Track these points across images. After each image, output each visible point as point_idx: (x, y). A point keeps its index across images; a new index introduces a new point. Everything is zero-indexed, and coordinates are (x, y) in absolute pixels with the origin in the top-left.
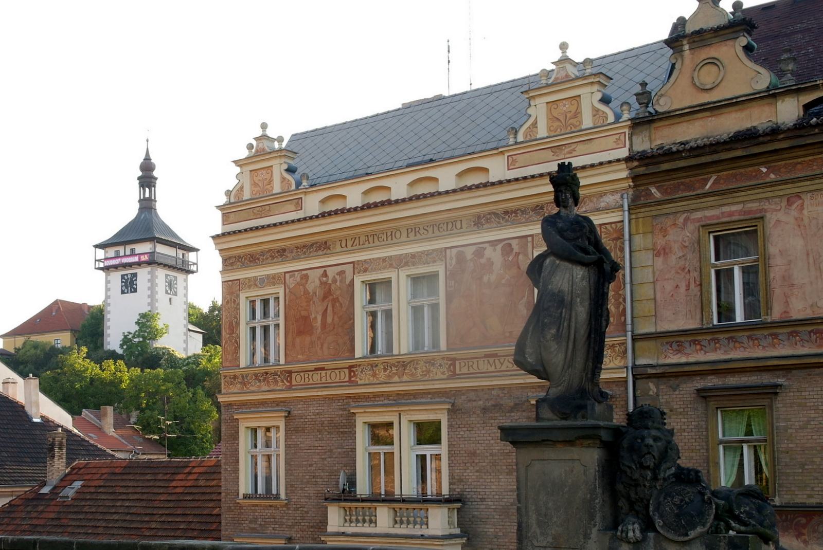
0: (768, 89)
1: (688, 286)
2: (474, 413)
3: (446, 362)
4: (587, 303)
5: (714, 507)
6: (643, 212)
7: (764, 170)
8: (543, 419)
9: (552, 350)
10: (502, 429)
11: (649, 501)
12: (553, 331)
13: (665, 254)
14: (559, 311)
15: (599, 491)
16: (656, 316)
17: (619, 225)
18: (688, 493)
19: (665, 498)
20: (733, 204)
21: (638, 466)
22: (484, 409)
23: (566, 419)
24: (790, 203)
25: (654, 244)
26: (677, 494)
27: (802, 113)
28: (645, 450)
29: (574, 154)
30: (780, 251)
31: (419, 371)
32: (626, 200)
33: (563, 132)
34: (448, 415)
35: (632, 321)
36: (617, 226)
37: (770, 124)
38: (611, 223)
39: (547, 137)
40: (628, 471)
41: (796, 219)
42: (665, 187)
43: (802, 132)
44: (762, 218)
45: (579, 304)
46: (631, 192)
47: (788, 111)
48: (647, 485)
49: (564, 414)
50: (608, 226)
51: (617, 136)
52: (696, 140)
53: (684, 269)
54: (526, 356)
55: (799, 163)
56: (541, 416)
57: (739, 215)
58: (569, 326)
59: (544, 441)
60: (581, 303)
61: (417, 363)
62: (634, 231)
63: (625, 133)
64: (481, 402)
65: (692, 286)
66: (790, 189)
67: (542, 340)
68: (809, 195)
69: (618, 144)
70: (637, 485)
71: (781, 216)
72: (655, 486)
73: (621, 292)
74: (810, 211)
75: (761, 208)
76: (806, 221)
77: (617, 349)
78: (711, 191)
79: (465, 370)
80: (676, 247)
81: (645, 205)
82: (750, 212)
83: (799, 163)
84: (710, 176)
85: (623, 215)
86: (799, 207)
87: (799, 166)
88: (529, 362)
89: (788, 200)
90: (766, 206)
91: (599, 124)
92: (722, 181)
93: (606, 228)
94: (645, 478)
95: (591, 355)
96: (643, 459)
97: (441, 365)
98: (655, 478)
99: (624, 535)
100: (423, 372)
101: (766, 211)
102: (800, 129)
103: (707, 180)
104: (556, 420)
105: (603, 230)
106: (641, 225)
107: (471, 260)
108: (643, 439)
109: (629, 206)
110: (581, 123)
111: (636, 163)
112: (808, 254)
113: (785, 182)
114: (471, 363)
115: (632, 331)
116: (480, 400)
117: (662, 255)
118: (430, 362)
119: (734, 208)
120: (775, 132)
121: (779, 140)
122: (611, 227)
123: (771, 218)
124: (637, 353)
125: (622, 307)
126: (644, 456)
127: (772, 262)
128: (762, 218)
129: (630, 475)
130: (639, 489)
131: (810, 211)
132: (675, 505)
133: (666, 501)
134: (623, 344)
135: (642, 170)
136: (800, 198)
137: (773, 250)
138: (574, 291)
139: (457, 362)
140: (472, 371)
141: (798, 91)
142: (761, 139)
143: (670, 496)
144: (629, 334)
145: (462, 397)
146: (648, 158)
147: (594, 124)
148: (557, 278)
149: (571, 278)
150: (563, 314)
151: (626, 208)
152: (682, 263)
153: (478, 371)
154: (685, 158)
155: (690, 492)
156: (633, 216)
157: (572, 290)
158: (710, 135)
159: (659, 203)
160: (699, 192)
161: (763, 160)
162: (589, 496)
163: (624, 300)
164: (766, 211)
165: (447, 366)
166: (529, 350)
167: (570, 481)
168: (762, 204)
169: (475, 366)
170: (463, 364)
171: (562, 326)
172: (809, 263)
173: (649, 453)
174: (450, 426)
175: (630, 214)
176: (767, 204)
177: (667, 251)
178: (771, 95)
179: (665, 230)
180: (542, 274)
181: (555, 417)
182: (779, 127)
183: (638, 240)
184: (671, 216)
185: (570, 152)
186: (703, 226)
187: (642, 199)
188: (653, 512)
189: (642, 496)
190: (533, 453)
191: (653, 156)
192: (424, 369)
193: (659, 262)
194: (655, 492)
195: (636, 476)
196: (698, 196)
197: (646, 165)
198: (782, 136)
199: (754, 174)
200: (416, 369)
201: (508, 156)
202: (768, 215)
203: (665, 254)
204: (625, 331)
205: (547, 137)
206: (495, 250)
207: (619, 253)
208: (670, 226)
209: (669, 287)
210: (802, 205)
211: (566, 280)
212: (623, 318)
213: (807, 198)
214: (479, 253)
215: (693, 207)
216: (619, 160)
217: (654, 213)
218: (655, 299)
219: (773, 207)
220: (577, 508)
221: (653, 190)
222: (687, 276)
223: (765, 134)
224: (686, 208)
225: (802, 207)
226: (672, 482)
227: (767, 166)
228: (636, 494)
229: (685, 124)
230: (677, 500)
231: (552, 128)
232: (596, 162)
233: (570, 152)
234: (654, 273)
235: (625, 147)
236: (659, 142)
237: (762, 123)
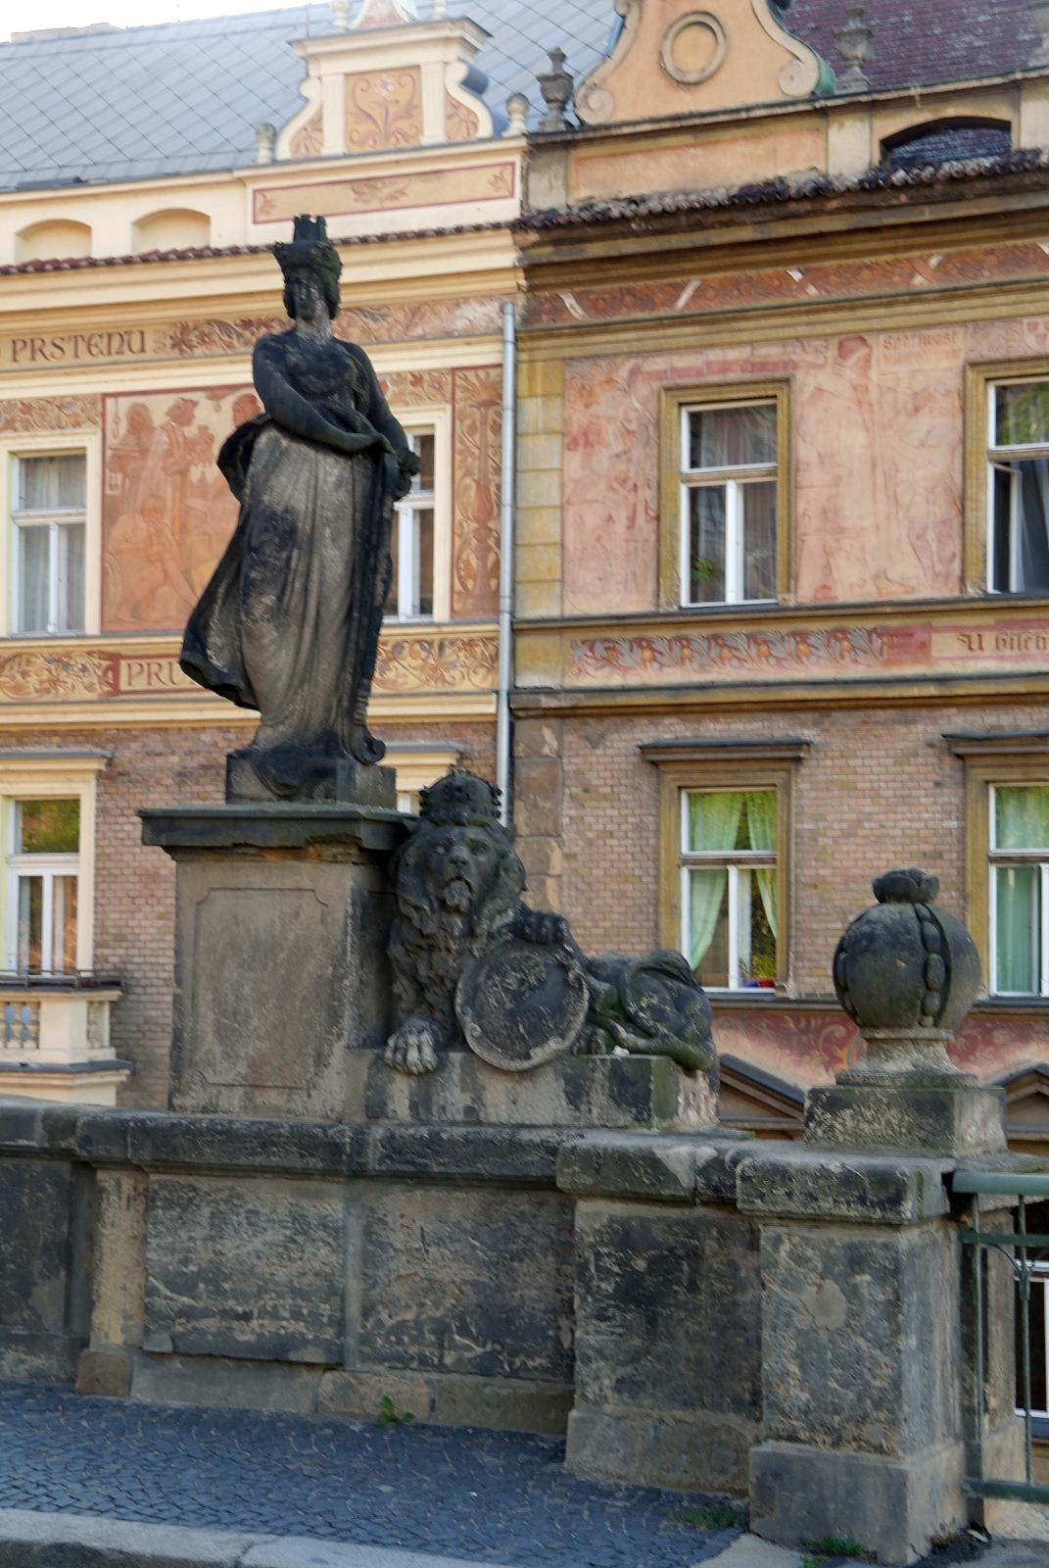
0: (813, 97)
1: (632, 520)
2: (158, 783)
3: (96, 661)
4: (346, 541)
5: (586, 995)
6: (547, 348)
7: (797, 276)
8: (240, 798)
9: (266, 641)
10: (147, 817)
11: (455, 983)
12: (269, 599)
13: (588, 444)
14: (284, 555)
15: (352, 959)
16: (562, 581)
17: (493, 372)
18: (537, 965)
19: (489, 977)
20: (732, 345)
21: (436, 905)
22: (180, 774)
23: (288, 798)
24: (843, 352)
25: (566, 422)
27: (877, 156)
28: (450, 871)
29: (403, 201)
30: (819, 455)
31: (33, 680)
32: (509, 318)
33: (379, 148)
34: (98, 785)
35: (513, 590)
36: (488, 374)
37: (813, 175)
38: (475, 368)
39: (345, 156)
40: (414, 915)
41: (855, 388)
42: (592, 297)
43: (875, 199)
44: (787, 381)
45: (328, 542)
46: (521, 300)
47: (850, 150)
48: (454, 947)
49: (288, 786)
50: (470, 375)
51: (497, 171)
52: (661, 196)
53: (624, 482)
54: (209, 652)
55: (868, 267)
56: (237, 790)
57: (743, 371)
58: (306, 589)
59: (237, 845)
60: (334, 540)
61: (29, 662)
62: (523, 389)
63: (513, 164)
64: (175, 759)
65: (641, 519)
66: (845, 322)
67: (244, 618)
68: (882, 337)
69: (498, 189)
70: (432, 948)
71: (824, 379)
73: (491, 525)
74: (883, 374)
75: (785, 358)
76: (874, 394)
77: (478, 649)
78: (687, 312)
79: (140, 683)
80: (610, 431)
81: (549, 334)
82: (763, 366)
83: (868, 267)
84: (685, 279)
85: (503, 352)
86: (861, 363)
87: (866, 274)
88: (215, 668)
89: (841, 346)
90: (797, 354)
91: (459, 139)
92: (710, 293)
93: (466, 379)
94: (448, 933)
95: (351, 658)
96: (446, 891)
97: (84, 669)
98: (471, 933)
100: (41, 682)
101: (795, 366)
102: (870, 191)
103: (679, 288)
104: (269, 800)
105: (459, 381)
106: (539, 379)
107: (163, 428)
108: (449, 845)
109: (516, 331)
110: (419, 130)
111: (533, 237)
112: (874, 466)
113: (836, 306)
114: (154, 668)
115: (512, 613)
116: (173, 753)
117: (581, 449)
118: (59, 661)
119: (732, 355)
120: (820, 193)
121: (830, 213)
122: (477, 376)
123: (806, 381)
124: (521, 660)
125: (492, 557)
126: (447, 884)
127: (804, 478)
128: (787, 381)
130: (436, 956)
131: (883, 374)
132: (506, 990)
134: (492, 639)
135: (546, 253)
136: (863, 340)
137: (805, 452)
138: (318, 511)
139: (123, 664)
140: (156, 685)
141: (873, 107)
142: (793, 207)
144: (506, 618)
145: (134, 745)
146: (559, 225)
147: (448, 136)
148: (283, 479)
149: (313, 482)
150: (293, 564)
151: (510, 335)
152: (622, 467)
153: (171, 686)
154: (636, 234)
155: (540, 961)
156: (524, 356)
157: (314, 510)
158: (689, 187)
159: (581, 330)
160: (662, 312)
161: (795, 253)
162: (330, 971)
163: (498, 543)
164: (795, 366)
165: (100, 673)
166: (215, 639)
167: (291, 936)
168: (790, 349)
169: (164, 675)
170: (136, 668)
171: (289, 588)
172: (874, 484)
173: (459, 878)
174: (102, 812)
175: (517, 349)
176: (799, 350)
177: (592, 438)
178: (820, 110)
179: (591, 393)
180: (251, 469)
181: (268, 794)
182: (830, 183)
183: (532, 409)
184: (603, 363)
185: (393, 197)
186: (668, 389)
187: (545, 317)
188: (462, 1007)
189: (441, 972)
190: (214, 873)
191: (570, 225)
192: (46, 675)
193: (575, 459)
194: (471, 963)
195: (431, 927)
196: (661, 323)
197: (556, 243)
198: (833, 204)
200: (24, 674)
201: (255, 192)
202: (800, 376)
203: (588, 444)
204: (497, 611)
205: (345, 156)
206: (218, 409)
207: (490, 436)
208: (600, 384)
209: (593, 518)
210: (867, 360)
211: (301, 485)
212: (493, 583)
213: (877, 344)
214: (182, 413)
215: (650, 344)
216: (497, 226)
217: (568, 352)
218: (562, 545)
219: (810, 358)
220: (304, 998)
221: (569, 301)
222: (631, 498)
223: (802, 197)
224: (636, 346)
225: (867, 363)
228: (431, 967)
229: (640, 158)
230: (512, 981)
231: (356, 137)
232: (449, 224)
233: (393, 197)
234: (563, 486)
235: (512, 195)
236: (583, 193)
237: (799, 172)
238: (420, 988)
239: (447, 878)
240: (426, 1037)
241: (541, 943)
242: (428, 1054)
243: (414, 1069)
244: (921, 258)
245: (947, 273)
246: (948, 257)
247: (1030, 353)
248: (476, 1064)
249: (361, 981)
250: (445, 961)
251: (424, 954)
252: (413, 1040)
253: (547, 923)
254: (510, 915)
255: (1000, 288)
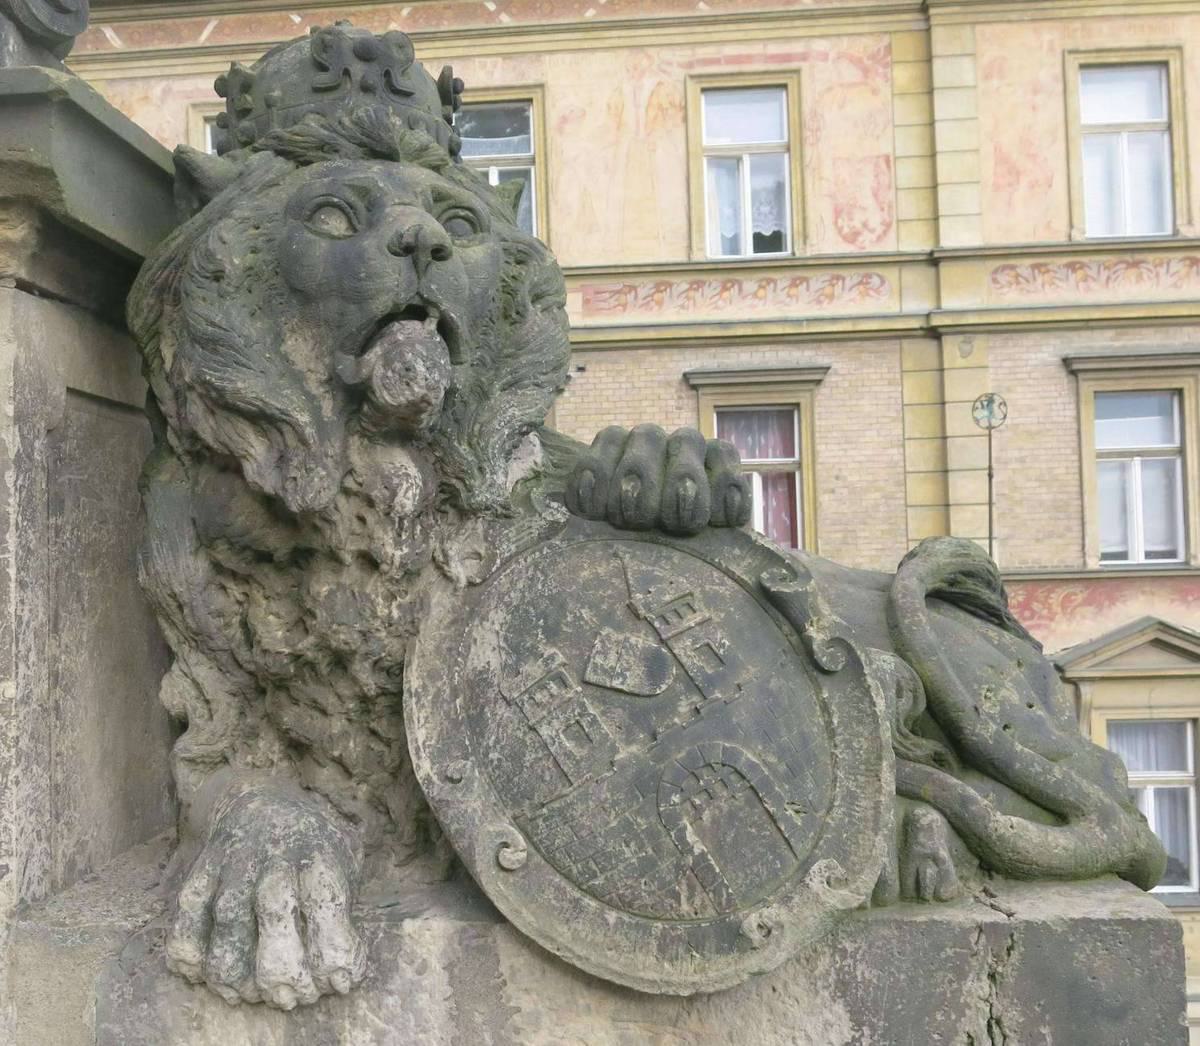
7: (297, 19)
18: (686, 602)
19: (517, 649)
21: (328, 407)
26: (607, 619)
40: (256, 450)
42: (130, 31)
48: (393, 552)
55: (354, 14)
70: (302, 558)
72: (441, 569)
78: (208, 44)
83: (354, 14)
84: (206, 18)
92: (227, 31)
96: (374, 355)
98: (450, 500)
99: (226, 957)
103: (202, 27)
108: (364, 209)
129: (270, 484)
130: (322, 586)
132: (605, 692)
133: (533, 669)
143: (552, 634)
173: (417, 312)
184: (140, 84)
186: (194, 106)
187: (89, 46)
188: (439, 755)
189: (344, 637)
194: (441, 602)
199: (280, 24)
226: (554, 528)
227: (301, 12)
228: (302, 620)
230: (620, 658)
238: (263, 686)
239: (381, 305)
240: (325, 880)
241: (669, 527)
242: (340, 951)
243: (286, 998)
244: (395, 9)
245: (415, 21)
246: (416, 10)
247: (481, 85)
248: (510, 959)
249: (55, 678)
250: (360, 599)
251: (276, 583)
252: (278, 897)
253: (690, 459)
254: (533, 455)
255: (457, 35)
